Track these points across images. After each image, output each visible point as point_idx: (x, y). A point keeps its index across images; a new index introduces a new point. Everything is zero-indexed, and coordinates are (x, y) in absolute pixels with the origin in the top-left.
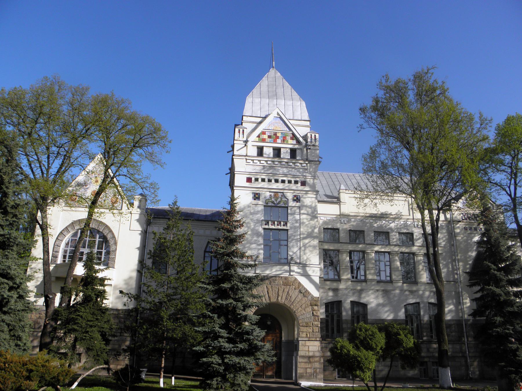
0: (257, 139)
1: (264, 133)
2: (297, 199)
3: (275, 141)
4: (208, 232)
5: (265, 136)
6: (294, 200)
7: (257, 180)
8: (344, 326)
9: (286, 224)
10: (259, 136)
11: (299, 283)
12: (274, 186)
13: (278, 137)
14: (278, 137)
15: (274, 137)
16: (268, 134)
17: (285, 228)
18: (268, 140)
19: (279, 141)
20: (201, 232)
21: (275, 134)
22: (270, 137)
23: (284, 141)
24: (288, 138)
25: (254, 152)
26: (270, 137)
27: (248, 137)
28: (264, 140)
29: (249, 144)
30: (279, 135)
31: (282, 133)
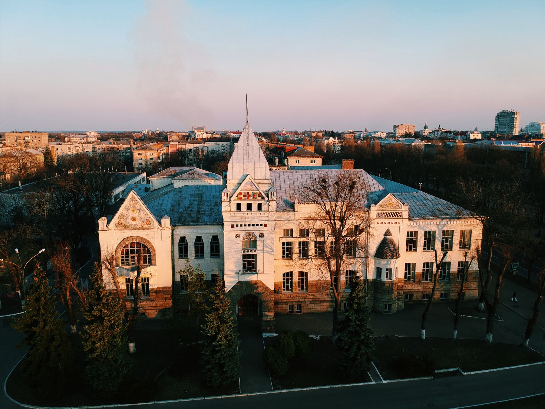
1: (241, 194)
2: (262, 236)
3: (248, 198)
4: (212, 231)
5: (242, 196)
6: (260, 236)
7: (237, 226)
8: (294, 285)
10: (237, 196)
12: (248, 228)
13: (250, 196)
14: (250, 196)
15: (247, 196)
16: (243, 194)
17: (255, 253)
18: (243, 198)
19: (251, 198)
20: (208, 231)
21: (248, 193)
22: (244, 196)
23: (254, 198)
24: (256, 196)
25: (234, 207)
26: (244, 196)
27: (230, 198)
28: (241, 199)
29: (232, 202)
30: (250, 194)
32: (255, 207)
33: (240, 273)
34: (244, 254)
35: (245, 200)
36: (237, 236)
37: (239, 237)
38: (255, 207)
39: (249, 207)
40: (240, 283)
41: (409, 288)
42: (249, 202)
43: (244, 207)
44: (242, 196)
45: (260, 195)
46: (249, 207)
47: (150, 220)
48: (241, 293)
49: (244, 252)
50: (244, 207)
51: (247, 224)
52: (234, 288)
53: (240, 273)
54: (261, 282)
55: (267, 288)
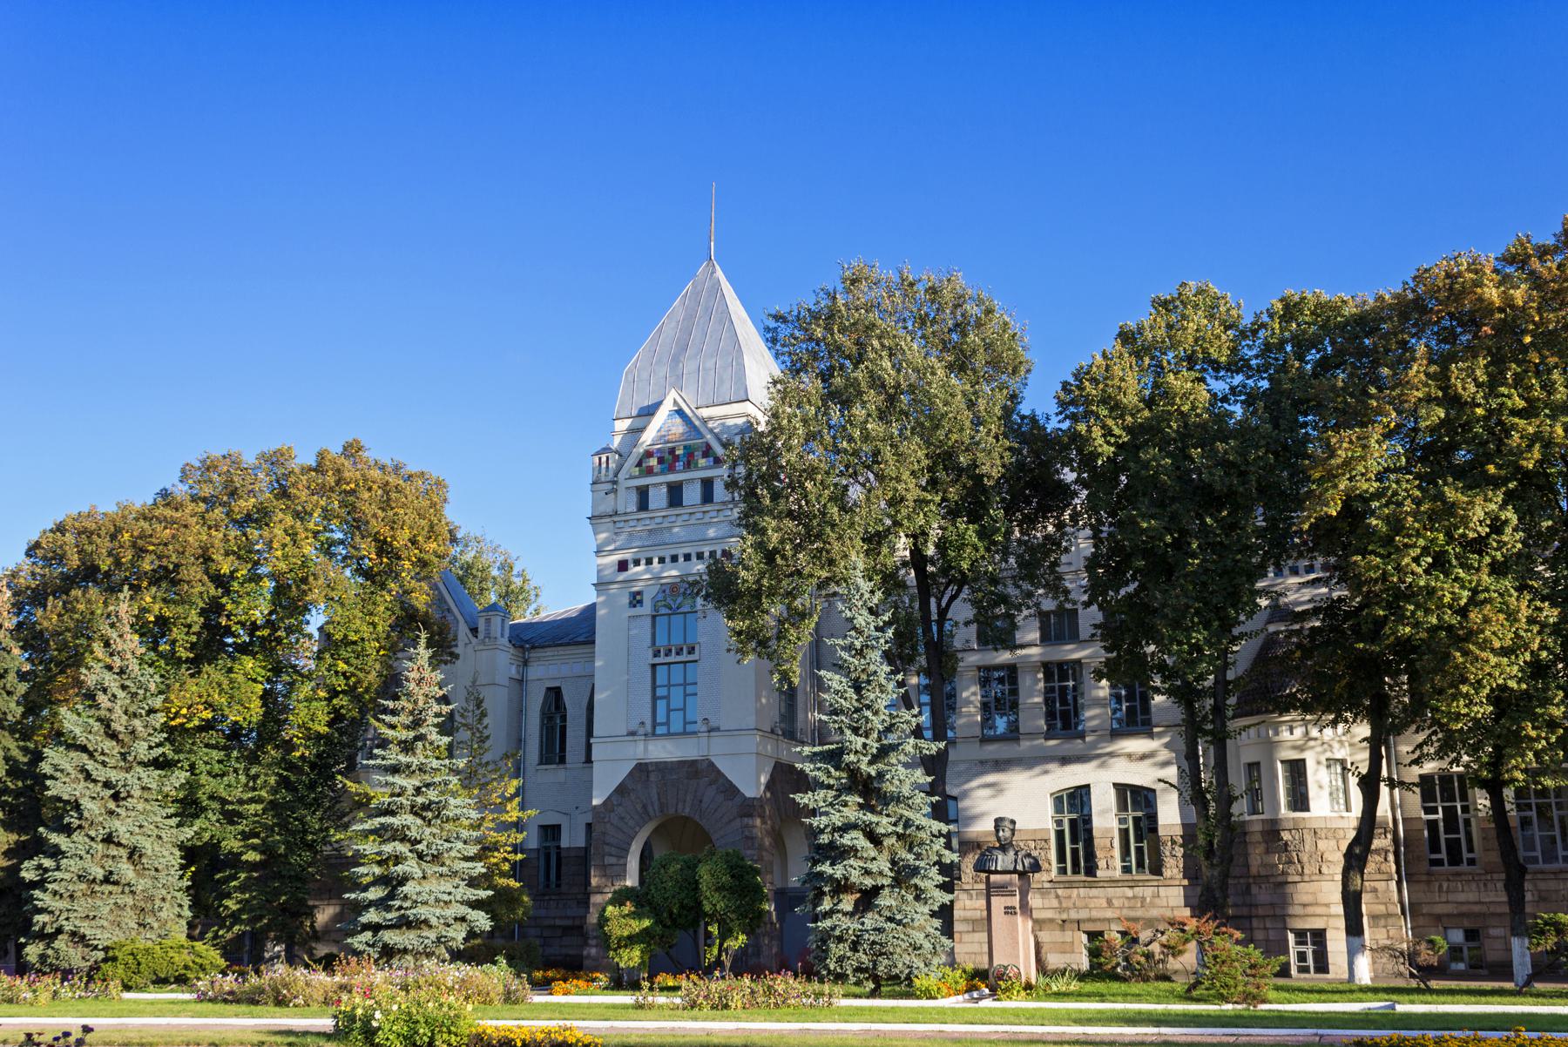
0: (636, 471)
1: (648, 454)
3: (671, 469)
9: (691, 650)
10: (639, 464)
11: (719, 771)
13: (676, 458)
14: (676, 458)
17: (691, 658)
21: (672, 451)
23: (689, 465)
24: (698, 454)
25: (629, 503)
26: (661, 461)
31: (685, 447)
32: (692, 494)
33: (641, 731)
34: (657, 660)
35: (662, 473)
36: (636, 600)
37: (640, 602)
38: (692, 494)
39: (675, 495)
40: (642, 770)
41: (1462, 897)
42: (672, 478)
43: (658, 498)
44: (653, 462)
45: (707, 451)
46: (675, 495)
47: (450, 618)
48: (644, 807)
49: (656, 654)
50: (658, 498)
51: (667, 554)
52: (621, 790)
53: (641, 731)
54: (712, 764)
55: (731, 790)
